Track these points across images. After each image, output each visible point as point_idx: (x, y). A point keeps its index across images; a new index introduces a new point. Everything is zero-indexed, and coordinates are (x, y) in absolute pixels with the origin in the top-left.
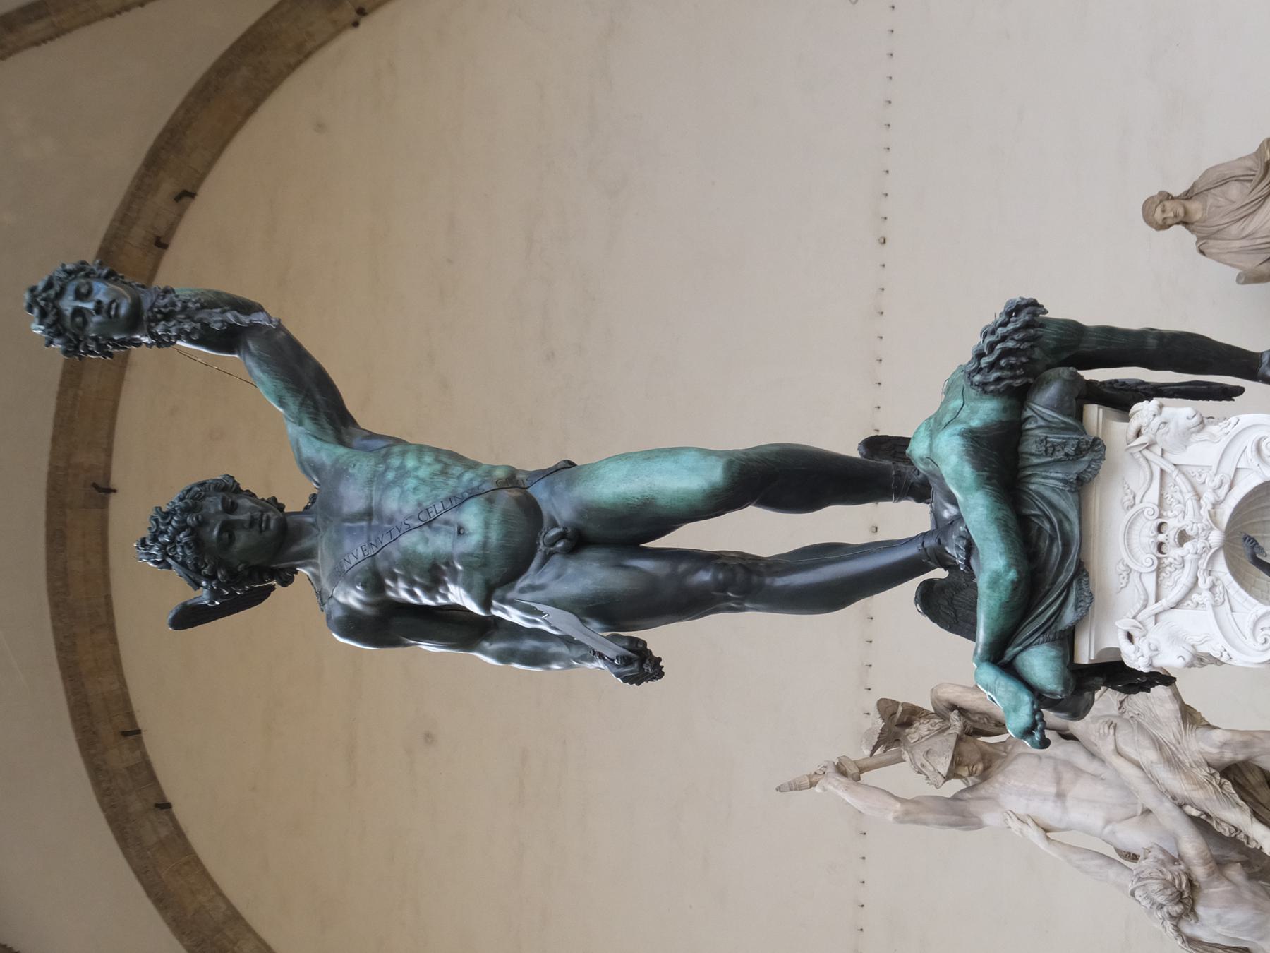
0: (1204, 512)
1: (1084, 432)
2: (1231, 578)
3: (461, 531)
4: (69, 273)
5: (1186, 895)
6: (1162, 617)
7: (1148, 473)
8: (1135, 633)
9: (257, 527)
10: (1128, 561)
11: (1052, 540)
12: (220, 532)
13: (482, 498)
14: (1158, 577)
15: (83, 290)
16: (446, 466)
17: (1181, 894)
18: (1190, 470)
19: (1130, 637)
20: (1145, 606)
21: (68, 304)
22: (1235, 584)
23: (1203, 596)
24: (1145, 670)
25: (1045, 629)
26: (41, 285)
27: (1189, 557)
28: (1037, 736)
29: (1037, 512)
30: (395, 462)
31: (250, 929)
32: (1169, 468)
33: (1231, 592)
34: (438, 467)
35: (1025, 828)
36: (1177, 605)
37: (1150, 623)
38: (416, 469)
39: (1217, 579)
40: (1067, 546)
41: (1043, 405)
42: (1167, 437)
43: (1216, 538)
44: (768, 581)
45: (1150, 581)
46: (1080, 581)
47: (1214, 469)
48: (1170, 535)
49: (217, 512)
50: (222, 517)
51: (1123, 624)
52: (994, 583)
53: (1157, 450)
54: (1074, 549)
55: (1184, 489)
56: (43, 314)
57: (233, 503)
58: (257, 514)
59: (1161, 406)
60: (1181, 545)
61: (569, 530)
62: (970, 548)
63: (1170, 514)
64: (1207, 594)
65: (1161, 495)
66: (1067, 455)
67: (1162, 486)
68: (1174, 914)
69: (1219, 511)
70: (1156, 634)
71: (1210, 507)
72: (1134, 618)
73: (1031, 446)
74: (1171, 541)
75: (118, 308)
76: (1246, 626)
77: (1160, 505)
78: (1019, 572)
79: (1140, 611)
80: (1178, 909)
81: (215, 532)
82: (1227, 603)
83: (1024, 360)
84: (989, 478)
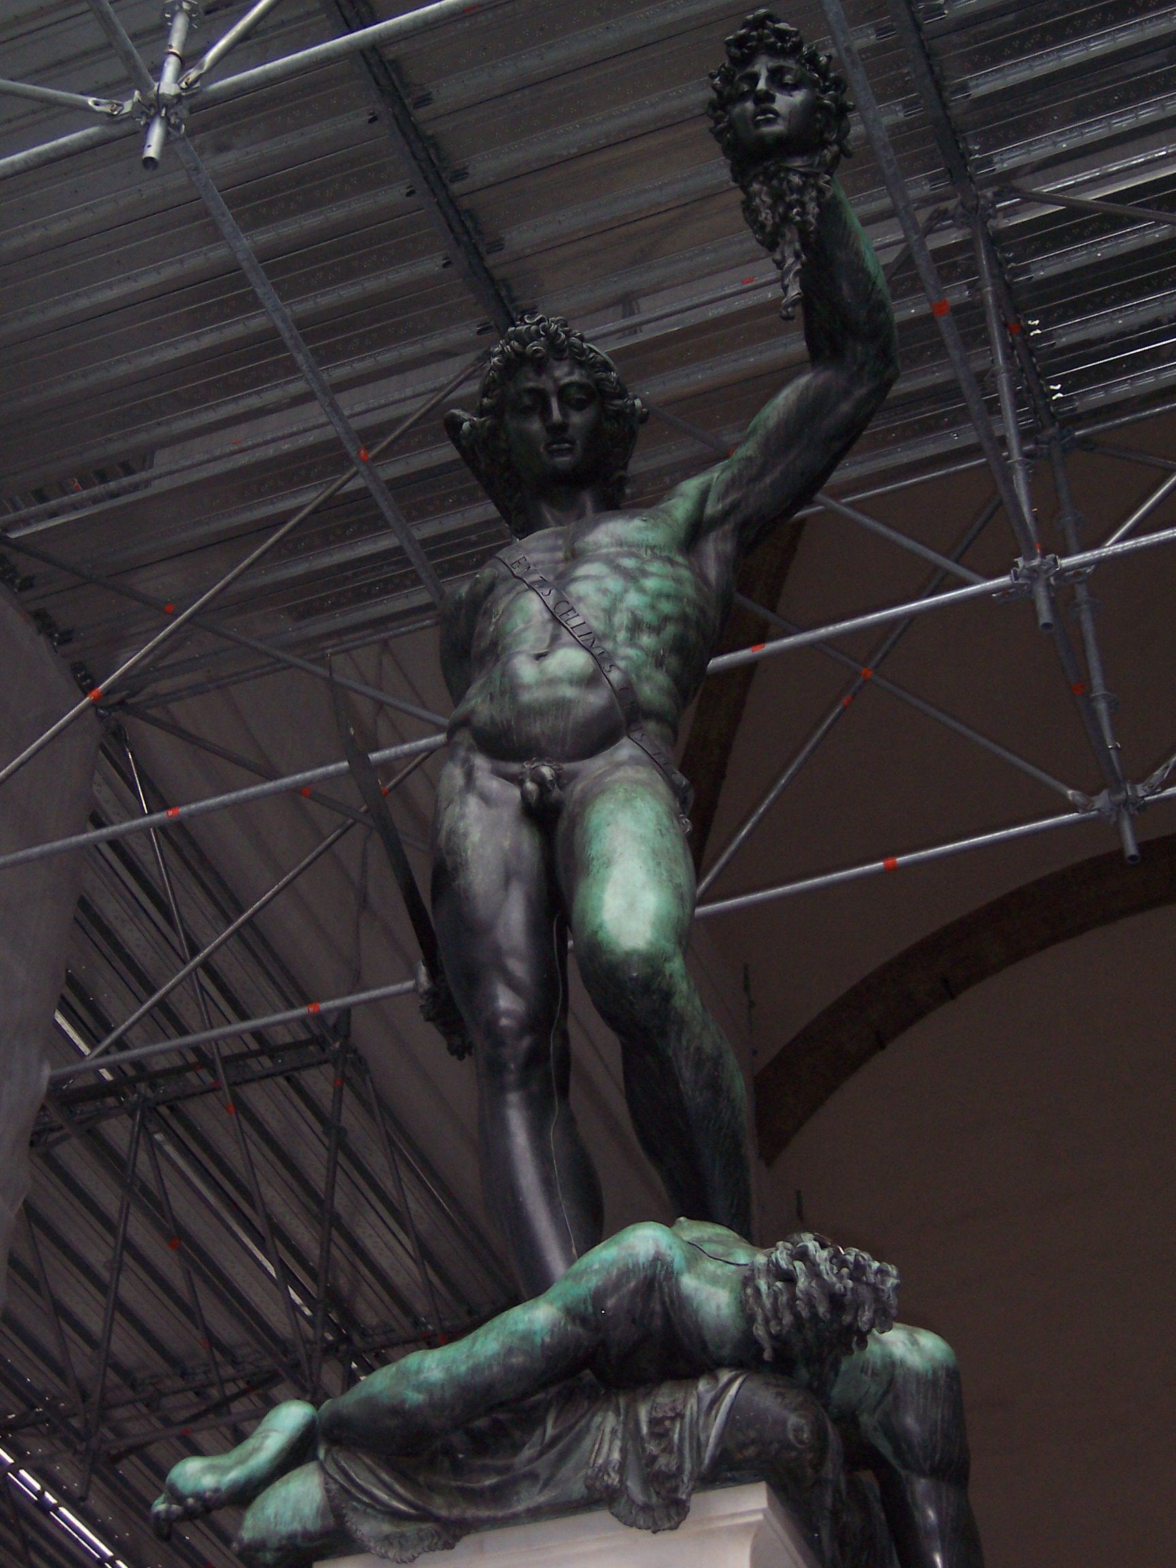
3: (539, 657)
4: (812, 59)
12: (531, 391)
15: (788, 78)
16: (656, 630)
21: (762, 66)
26: (782, 25)
29: (550, 1431)
30: (655, 567)
34: (648, 617)
38: (642, 590)
40: (497, 1495)
44: (513, 1098)
49: (556, 380)
50: (550, 386)
54: (484, 1513)
56: (740, 42)
66: (654, 1459)
75: (769, 122)
81: (531, 384)
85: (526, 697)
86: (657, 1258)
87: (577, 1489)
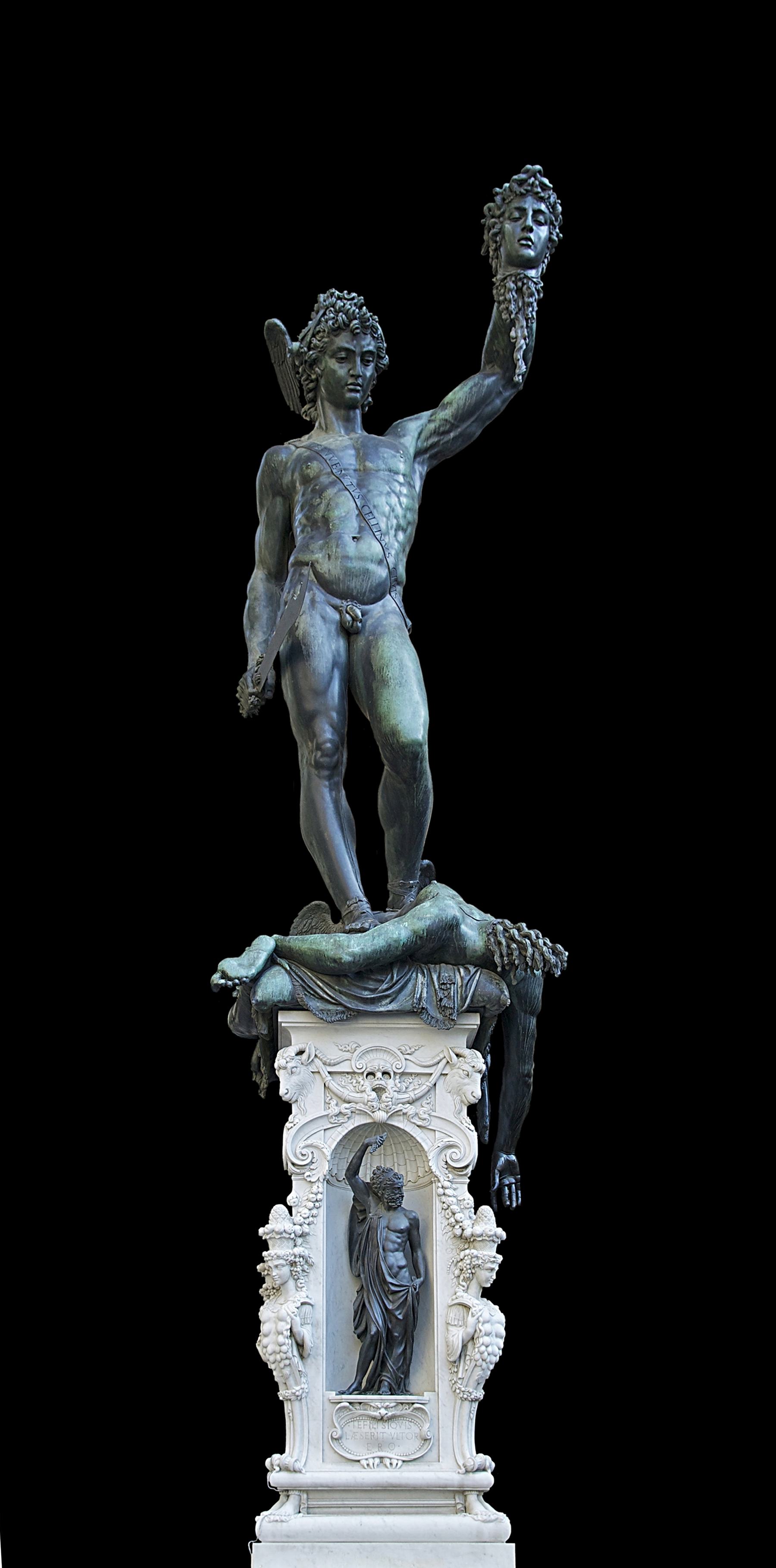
1: (460, 1014)
2: (350, 1129)
6: (317, 1075)
7: (428, 1063)
8: (304, 1056)
9: (350, 381)
10: (359, 1050)
11: (373, 991)
13: (381, 555)
14: (348, 1073)
18: (432, 1095)
19: (301, 1053)
20: (324, 1064)
22: (346, 1131)
24: (276, 1065)
25: (306, 988)
27: (364, 1095)
28: (223, 981)
32: (432, 1079)
33: (339, 1129)
37: (313, 1068)
40: (372, 1001)
41: (479, 983)
42: (457, 1078)
43: (381, 1116)
45: (344, 1067)
46: (343, 1012)
47: (433, 1114)
48: (379, 1080)
52: (339, 946)
55: (416, 1092)
57: (369, 361)
58: (360, 381)
59: (480, 1072)
60: (374, 1090)
61: (360, 625)
62: (362, 930)
63: (397, 1081)
64: (337, 1111)
65: (411, 1074)
66: (441, 1000)
67: (418, 1074)
69: (401, 1118)
70: (304, 1073)
71: (405, 1111)
73: (447, 972)
74: (377, 1082)
77: (403, 1074)
78: (350, 963)
83: (516, 962)
84: (421, 938)
85: (350, 565)
86: (454, 918)
87: (408, 1006)
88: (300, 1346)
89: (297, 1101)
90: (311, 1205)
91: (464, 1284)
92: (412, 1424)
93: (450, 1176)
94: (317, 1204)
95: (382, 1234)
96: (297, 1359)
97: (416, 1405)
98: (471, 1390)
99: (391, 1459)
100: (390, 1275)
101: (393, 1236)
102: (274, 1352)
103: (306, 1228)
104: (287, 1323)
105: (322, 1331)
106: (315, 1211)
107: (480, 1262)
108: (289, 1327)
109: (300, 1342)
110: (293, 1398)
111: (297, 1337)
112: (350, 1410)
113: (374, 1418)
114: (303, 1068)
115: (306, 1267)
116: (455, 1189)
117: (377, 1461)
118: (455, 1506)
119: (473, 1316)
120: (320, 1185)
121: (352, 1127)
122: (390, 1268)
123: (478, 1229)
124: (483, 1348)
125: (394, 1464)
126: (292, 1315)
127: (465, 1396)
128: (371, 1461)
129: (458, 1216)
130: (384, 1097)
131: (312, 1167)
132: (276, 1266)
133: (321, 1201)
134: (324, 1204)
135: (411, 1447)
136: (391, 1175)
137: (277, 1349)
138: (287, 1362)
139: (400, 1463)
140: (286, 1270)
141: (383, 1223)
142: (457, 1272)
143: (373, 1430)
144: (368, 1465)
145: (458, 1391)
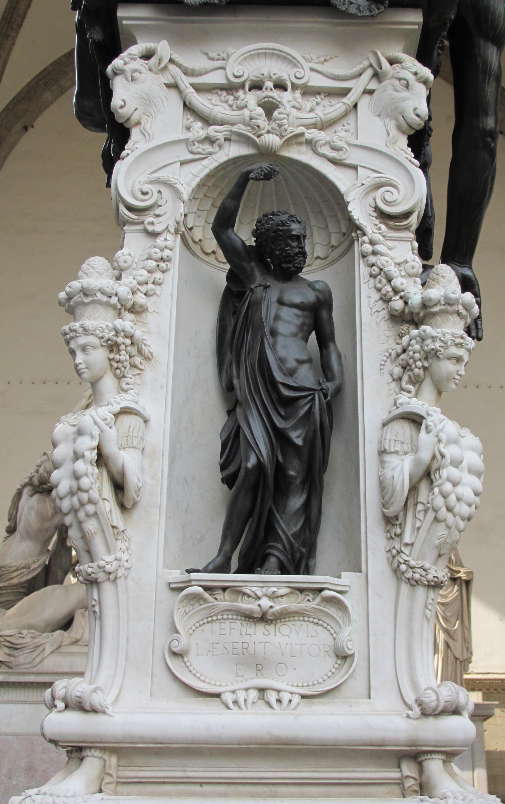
0: (301, 129)
5: (45, 486)
6: (173, 93)
8: (153, 60)
14: (222, 88)
17: (45, 484)
20: (186, 72)
22: (216, 164)
23: (199, 130)
31: (57, 97)
33: (205, 162)
35: (86, 398)
36: (187, 107)
37: (167, 78)
39: (220, 147)
42: (390, 91)
51: (164, 48)
53: (373, 85)
64: (202, 134)
68: (33, 479)
69: (304, 148)
70: (151, 82)
71: (308, 136)
72: (171, 61)
76: (162, 175)
79: (179, 66)
80: (36, 482)
82: (191, 157)
88: (119, 487)
89: (138, 123)
90: (152, 264)
91: (410, 387)
92: (320, 628)
93: (383, 227)
94: (162, 264)
95: (269, 310)
96: (108, 505)
97: (326, 593)
98: (427, 565)
99: (278, 691)
100: (281, 369)
101: (287, 313)
102: (72, 493)
103: (140, 298)
104: (92, 437)
105: (163, 464)
106: (158, 275)
107: (438, 344)
108: (95, 443)
109: (117, 477)
110: (101, 576)
111: (111, 465)
112: (205, 601)
113: (248, 617)
114: (151, 75)
115: (137, 360)
116: (390, 249)
117: (253, 695)
118: (400, 783)
119: (428, 431)
120: (170, 237)
121: (225, 159)
122: (282, 361)
123: (435, 293)
124: (448, 487)
125: (285, 701)
126: (102, 424)
127: (417, 576)
128: (241, 696)
129: (398, 282)
130: (276, 113)
131: (158, 211)
132: (84, 349)
133: (169, 260)
134: (175, 266)
135: (320, 671)
136: (284, 218)
137: (74, 484)
138: (90, 508)
139: (296, 699)
140: (99, 356)
141: (273, 295)
142: (398, 370)
143: (246, 638)
144: (235, 702)
145: (403, 567)
